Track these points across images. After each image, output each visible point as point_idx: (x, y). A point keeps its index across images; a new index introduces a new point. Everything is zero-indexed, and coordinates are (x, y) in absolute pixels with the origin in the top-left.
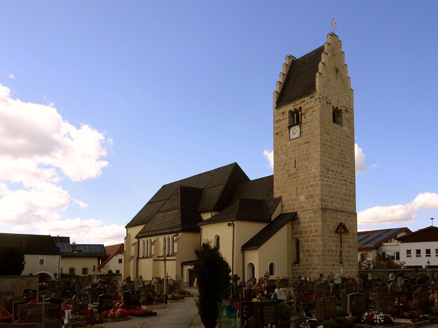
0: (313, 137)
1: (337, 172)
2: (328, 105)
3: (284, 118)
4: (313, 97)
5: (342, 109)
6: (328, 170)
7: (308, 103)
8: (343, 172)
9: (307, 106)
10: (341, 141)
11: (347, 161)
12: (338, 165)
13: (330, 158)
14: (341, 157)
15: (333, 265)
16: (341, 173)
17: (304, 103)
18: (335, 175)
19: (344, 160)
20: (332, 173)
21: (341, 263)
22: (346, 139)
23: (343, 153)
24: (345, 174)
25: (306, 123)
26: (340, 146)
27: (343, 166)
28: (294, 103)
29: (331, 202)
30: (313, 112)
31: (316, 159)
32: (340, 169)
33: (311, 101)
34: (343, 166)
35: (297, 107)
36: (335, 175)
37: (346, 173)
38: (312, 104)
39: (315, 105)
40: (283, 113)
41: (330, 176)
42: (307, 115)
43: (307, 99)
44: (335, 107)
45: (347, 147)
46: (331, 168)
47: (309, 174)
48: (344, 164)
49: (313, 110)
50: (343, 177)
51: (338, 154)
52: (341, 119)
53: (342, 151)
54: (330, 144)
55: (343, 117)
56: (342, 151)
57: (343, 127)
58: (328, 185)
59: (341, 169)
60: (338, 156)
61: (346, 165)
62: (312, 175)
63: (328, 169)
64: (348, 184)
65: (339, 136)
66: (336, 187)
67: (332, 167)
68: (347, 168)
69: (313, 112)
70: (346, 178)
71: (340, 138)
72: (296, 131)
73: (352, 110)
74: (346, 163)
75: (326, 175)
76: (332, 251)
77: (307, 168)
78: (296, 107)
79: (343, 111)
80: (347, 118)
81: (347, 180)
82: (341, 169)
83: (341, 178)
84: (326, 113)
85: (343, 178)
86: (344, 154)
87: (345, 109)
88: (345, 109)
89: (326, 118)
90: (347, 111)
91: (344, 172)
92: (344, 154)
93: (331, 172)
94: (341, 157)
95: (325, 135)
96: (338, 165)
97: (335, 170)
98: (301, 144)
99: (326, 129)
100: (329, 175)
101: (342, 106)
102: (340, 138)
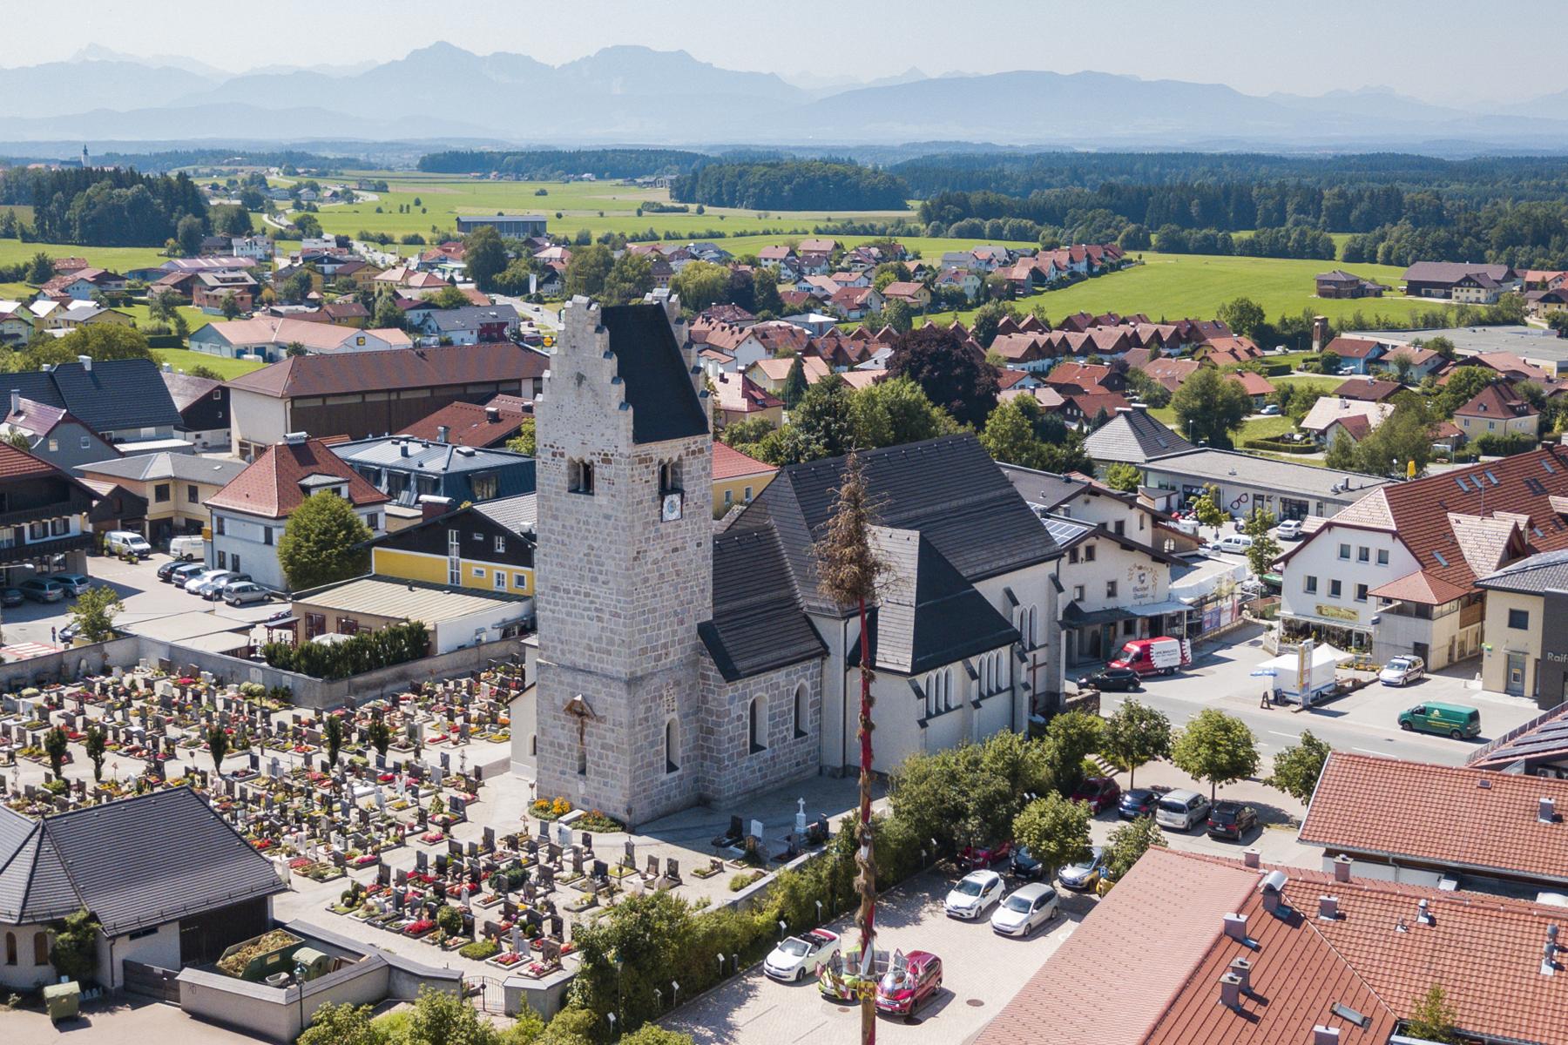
1: (577, 593)
5: (595, 458)
6: (556, 588)
13: (562, 566)
14: (589, 562)
15: (563, 773)
16: (587, 595)
19: (595, 568)
21: (583, 771)
22: (603, 521)
27: (594, 580)
29: (563, 652)
32: (586, 586)
34: (594, 580)
58: (554, 619)
60: (580, 560)
61: (601, 578)
64: (606, 616)
66: (573, 624)
76: (561, 746)
90: (607, 461)
94: (589, 562)
95: (549, 521)
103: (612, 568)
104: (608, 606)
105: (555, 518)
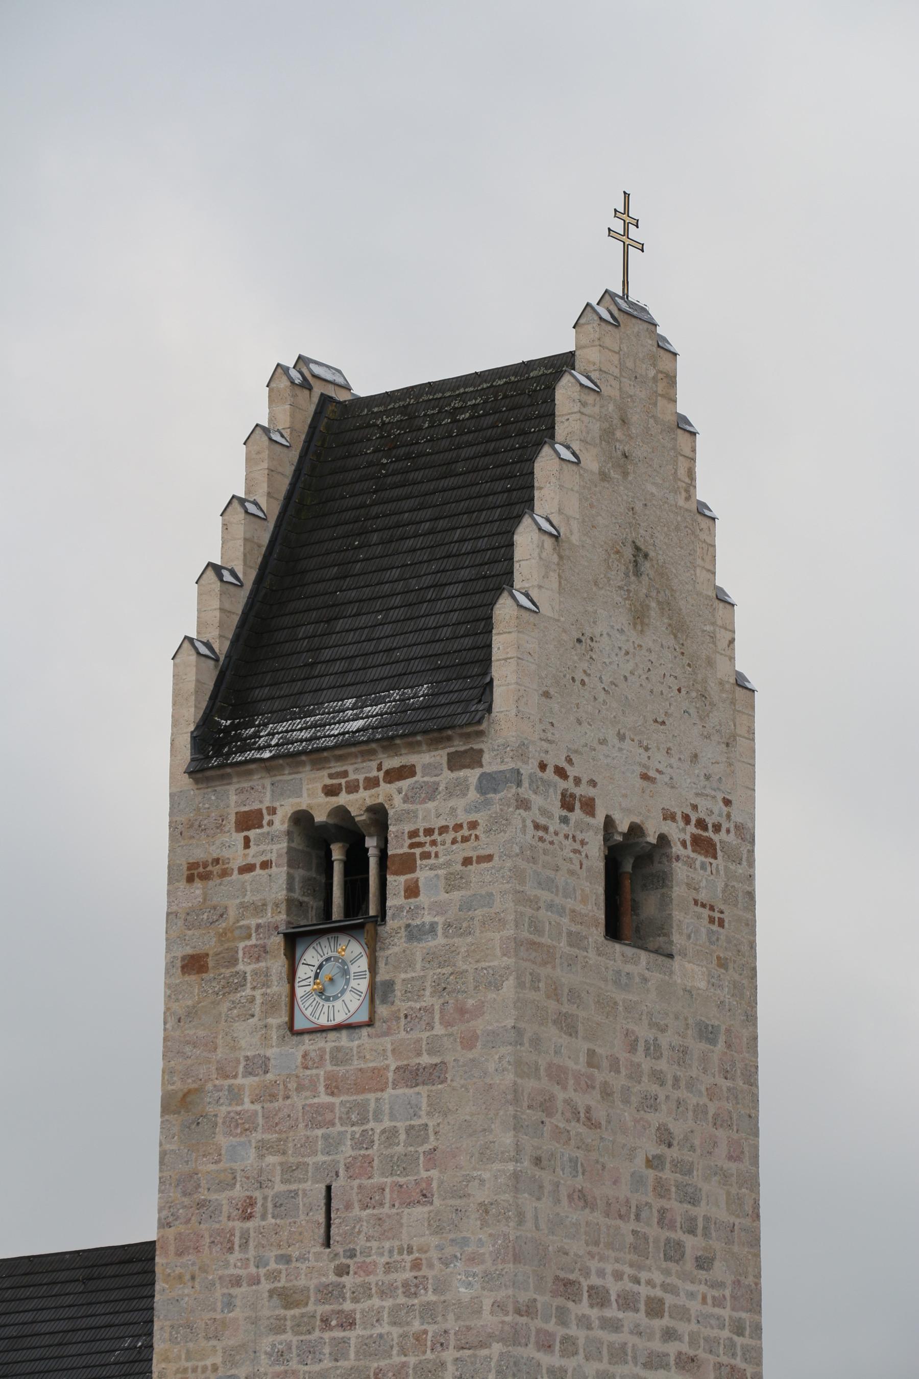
0: (469, 1042)
1: (627, 1302)
2: (577, 815)
3: (253, 855)
4: (473, 759)
5: (676, 832)
6: (567, 1288)
7: (432, 792)
8: (669, 1299)
9: (430, 813)
10: (662, 1065)
11: (700, 1212)
12: (640, 1245)
13: (583, 1199)
14: (661, 1189)
16: (655, 1308)
17: (405, 784)
18: (614, 1326)
20: (594, 1313)
22: (697, 1047)
23: (673, 1153)
24: (682, 1314)
25: (414, 934)
26: (650, 1103)
27: (674, 1252)
28: (338, 768)
30: (467, 861)
31: (485, 1209)
32: (654, 1277)
33: (459, 788)
34: (674, 1252)
35: (356, 803)
36: (614, 1326)
37: (695, 1306)
38: (459, 803)
39: (480, 817)
40: (248, 821)
41: (580, 1334)
42: (423, 875)
43: (428, 760)
44: (623, 827)
45: (700, 1111)
46: (586, 1273)
47: (429, 1312)
48: (679, 1235)
49: (467, 850)
50: (669, 1335)
51: (640, 1161)
52: (665, 902)
53: (666, 1138)
54: (581, 1100)
55: (678, 891)
56: (666, 1138)
57: (677, 963)
59: (658, 1277)
60: (638, 1181)
61: (692, 1244)
62: (451, 1324)
63: (568, 1283)
65: (644, 1032)
67: (594, 1265)
68: (704, 1263)
69: (467, 861)
70: (693, 1342)
71: (653, 1050)
72: (337, 981)
73: (746, 834)
74: (692, 1231)
75: (551, 1326)
77: (416, 1265)
78: (343, 799)
79: (677, 849)
80: (703, 896)
81: (702, 1354)
82: (658, 1277)
83: (657, 1345)
84: (561, 878)
85: (672, 1348)
86: (677, 1166)
87: (692, 829)
88: (692, 829)
89: (561, 911)
91: (682, 1300)
92: (677, 1166)
93: (584, 1307)
95: (552, 1034)
96: (640, 1245)
97: (614, 1289)
98: (374, 1080)
99: (554, 992)
100: (573, 1330)
101: (671, 817)
102: (653, 1050)
103: (722, 1214)
104: (712, 1344)
105: (571, 1031)
